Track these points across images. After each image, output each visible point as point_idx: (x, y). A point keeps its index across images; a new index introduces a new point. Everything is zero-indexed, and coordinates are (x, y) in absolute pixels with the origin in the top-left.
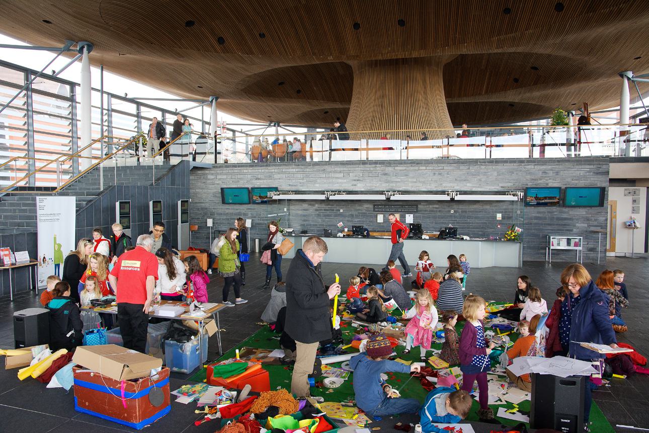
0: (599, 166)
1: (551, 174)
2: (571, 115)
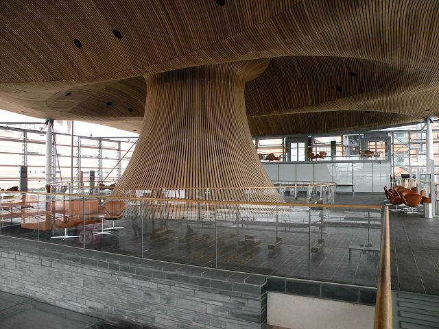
0: (241, 300)
1: (157, 299)
2: (429, 121)
